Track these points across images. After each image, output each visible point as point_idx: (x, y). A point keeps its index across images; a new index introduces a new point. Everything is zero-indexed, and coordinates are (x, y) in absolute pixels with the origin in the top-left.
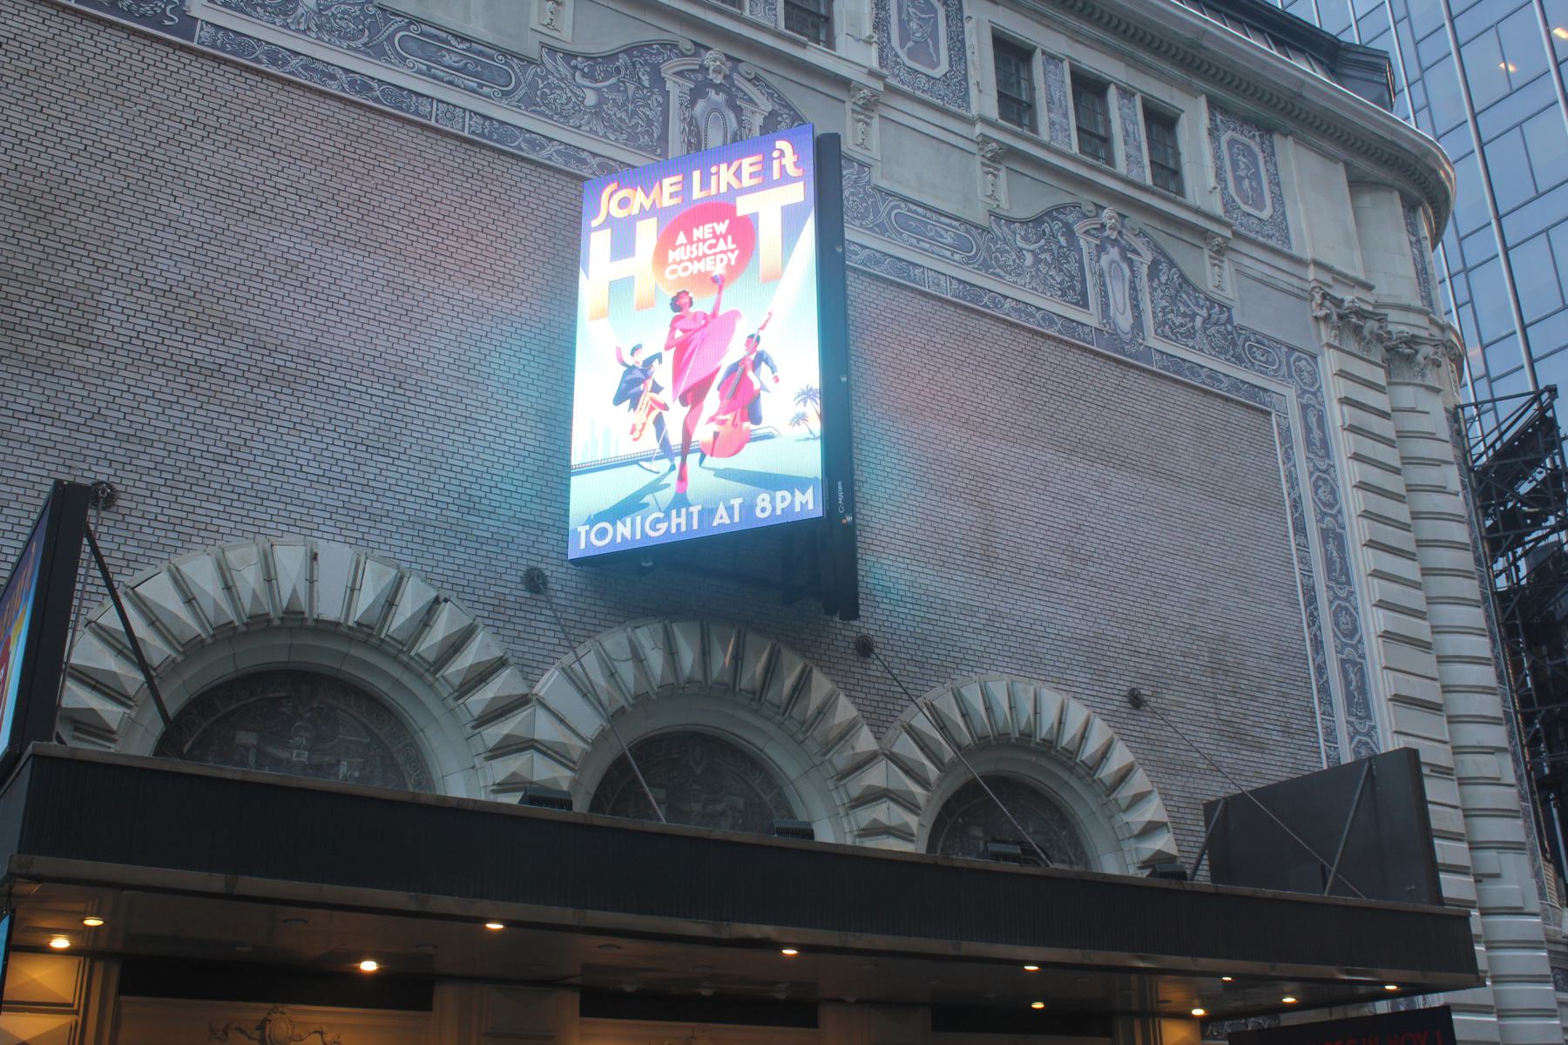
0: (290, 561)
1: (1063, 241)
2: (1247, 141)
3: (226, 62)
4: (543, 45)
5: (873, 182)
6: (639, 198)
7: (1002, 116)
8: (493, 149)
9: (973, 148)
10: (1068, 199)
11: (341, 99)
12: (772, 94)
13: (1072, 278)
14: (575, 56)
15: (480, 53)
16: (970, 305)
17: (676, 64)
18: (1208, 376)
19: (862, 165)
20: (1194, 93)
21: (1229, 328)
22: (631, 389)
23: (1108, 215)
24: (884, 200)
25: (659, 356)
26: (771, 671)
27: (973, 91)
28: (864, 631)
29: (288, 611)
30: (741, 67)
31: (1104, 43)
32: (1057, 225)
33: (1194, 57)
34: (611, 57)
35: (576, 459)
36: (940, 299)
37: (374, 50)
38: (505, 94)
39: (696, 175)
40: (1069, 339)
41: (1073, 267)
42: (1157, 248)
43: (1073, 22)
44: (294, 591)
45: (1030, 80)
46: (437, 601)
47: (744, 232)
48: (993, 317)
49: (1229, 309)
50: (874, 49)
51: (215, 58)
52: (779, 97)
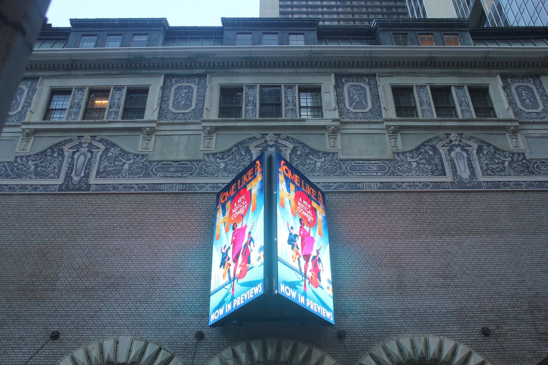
0: (108, 346)
1: (431, 153)
2: (524, 84)
3: (100, 194)
4: (204, 154)
5: (339, 158)
7: (398, 115)
8: (187, 193)
9: (385, 132)
10: (432, 136)
11: (135, 194)
12: (293, 141)
13: (436, 165)
14: (216, 154)
15: (183, 164)
16: (386, 190)
17: (255, 143)
18: (514, 185)
19: (333, 154)
20: (494, 75)
21: (524, 161)
23: (453, 136)
24: (344, 163)
25: (229, 248)
26: (294, 353)
27: (383, 110)
28: (340, 329)
29: (107, 362)
30: (281, 136)
31: (444, 73)
32: (427, 148)
33: (489, 63)
34: (230, 150)
35: (212, 289)
36: (372, 192)
37: (147, 175)
38: (190, 174)
39: (239, 181)
40: (437, 189)
41: (437, 161)
42: (481, 141)
43: (428, 70)
44: (109, 355)
45: (414, 98)
46: (160, 349)
48: (397, 192)
49: (523, 154)
50: (337, 112)
51: (97, 194)
52: (297, 141)
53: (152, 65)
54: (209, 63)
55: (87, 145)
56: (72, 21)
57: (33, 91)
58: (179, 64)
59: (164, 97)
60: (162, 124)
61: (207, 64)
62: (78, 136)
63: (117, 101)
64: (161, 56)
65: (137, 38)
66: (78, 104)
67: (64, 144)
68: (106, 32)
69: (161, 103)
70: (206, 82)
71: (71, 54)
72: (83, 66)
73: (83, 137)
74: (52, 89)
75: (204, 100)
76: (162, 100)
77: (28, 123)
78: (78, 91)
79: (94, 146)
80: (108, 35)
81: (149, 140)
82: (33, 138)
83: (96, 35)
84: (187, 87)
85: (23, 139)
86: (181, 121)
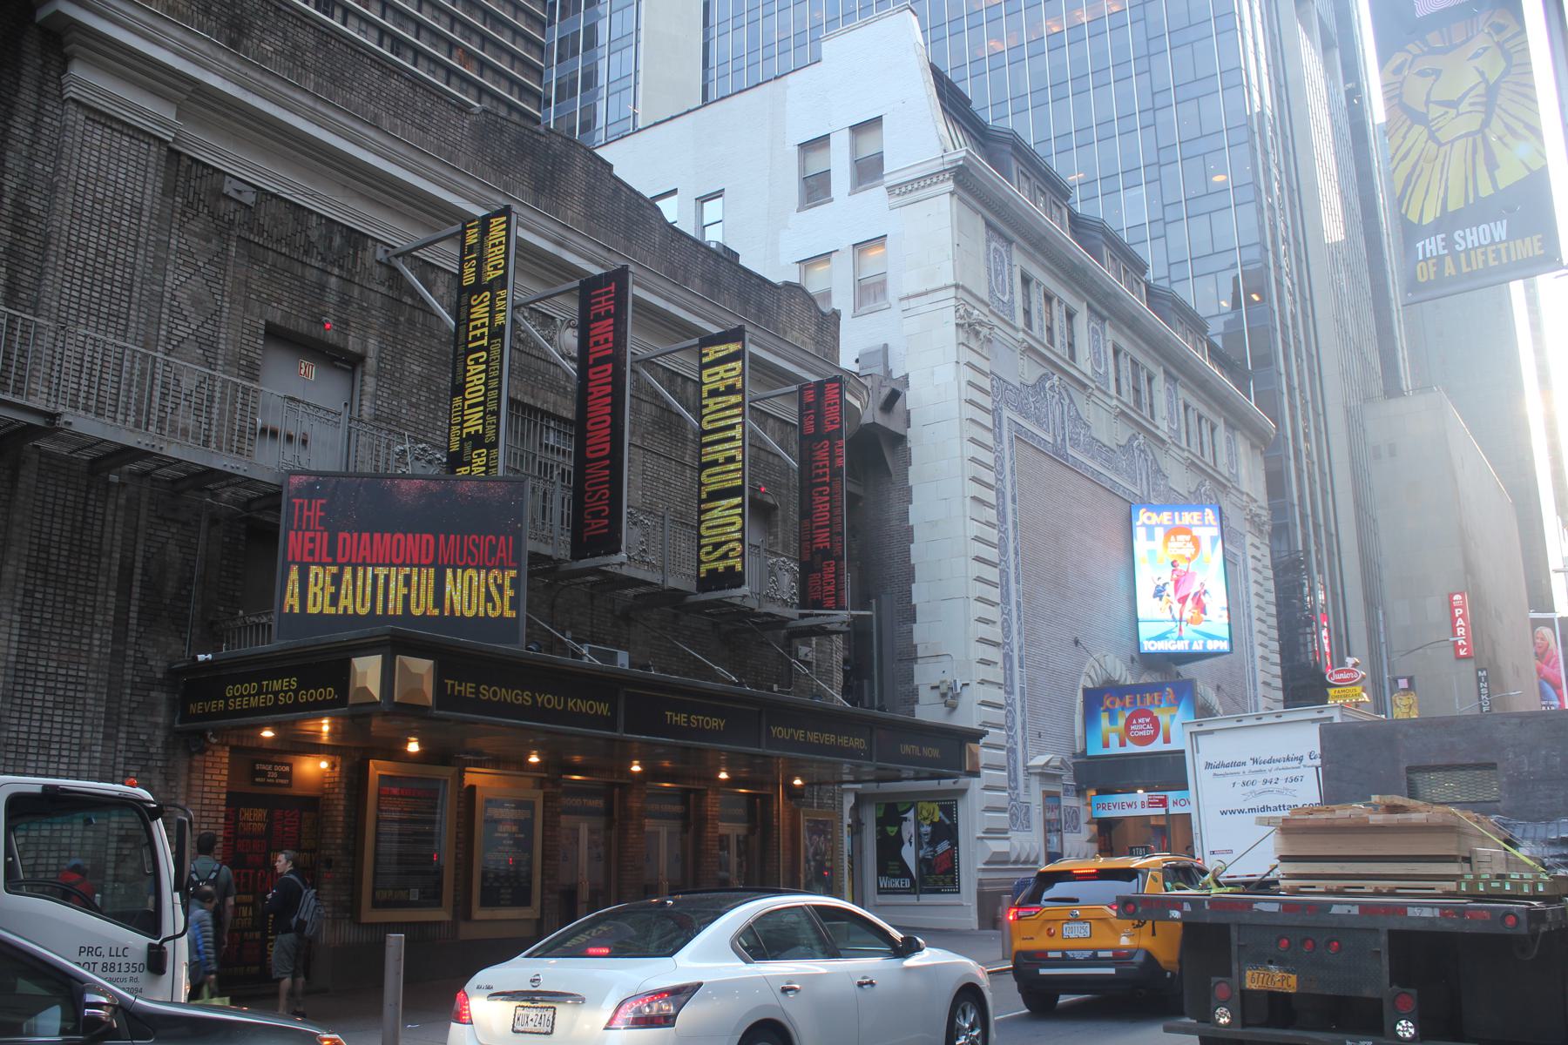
6: (1155, 518)
22: (1159, 593)
37: (1093, 457)
47: (1196, 542)
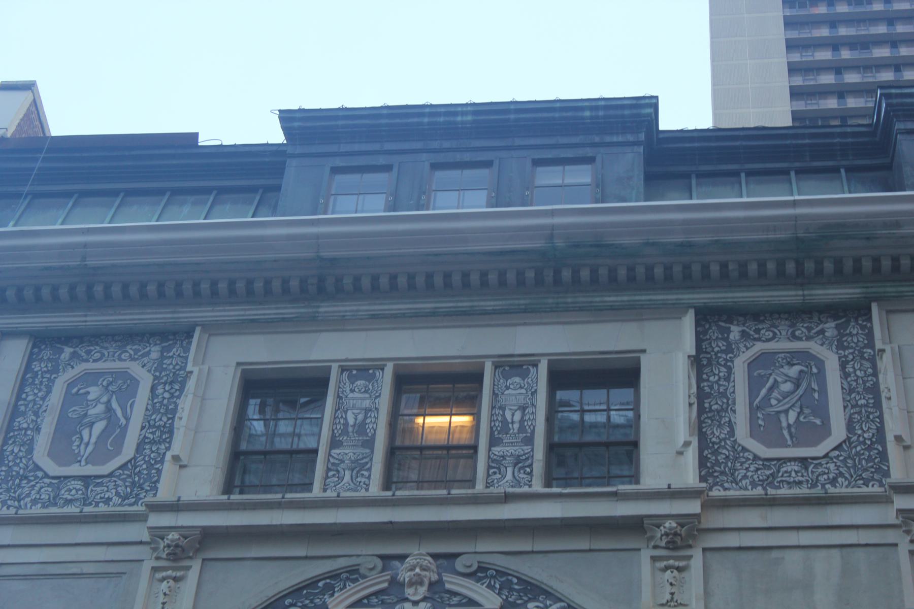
53: (640, 271)
54: (876, 260)
55: (423, 591)
56: (287, 118)
57: (173, 382)
58: (753, 267)
59: (709, 395)
60: (726, 504)
61: (867, 264)
62: (383, 557)
63: (518, 417)
64: (679, 239)
65: (548, 177)
66: (361, 428)
67: (330, 589)
68: (424, 156)
69: (700, 423)
70: (870, 335)
71: (317, 237)
72: (366, 282)
73: (402, 558)
74: (244, 372)
75: (878, 405)
76: (701, 410)
77: (176, 507)
78: (352, 379)
79: (456, 594)
80: (435, 166)
81: (679, 569)
82: (196, 565)
83: (387, 168)
84: (793, 357)
85: (155, 569)
86: (797, 491)
